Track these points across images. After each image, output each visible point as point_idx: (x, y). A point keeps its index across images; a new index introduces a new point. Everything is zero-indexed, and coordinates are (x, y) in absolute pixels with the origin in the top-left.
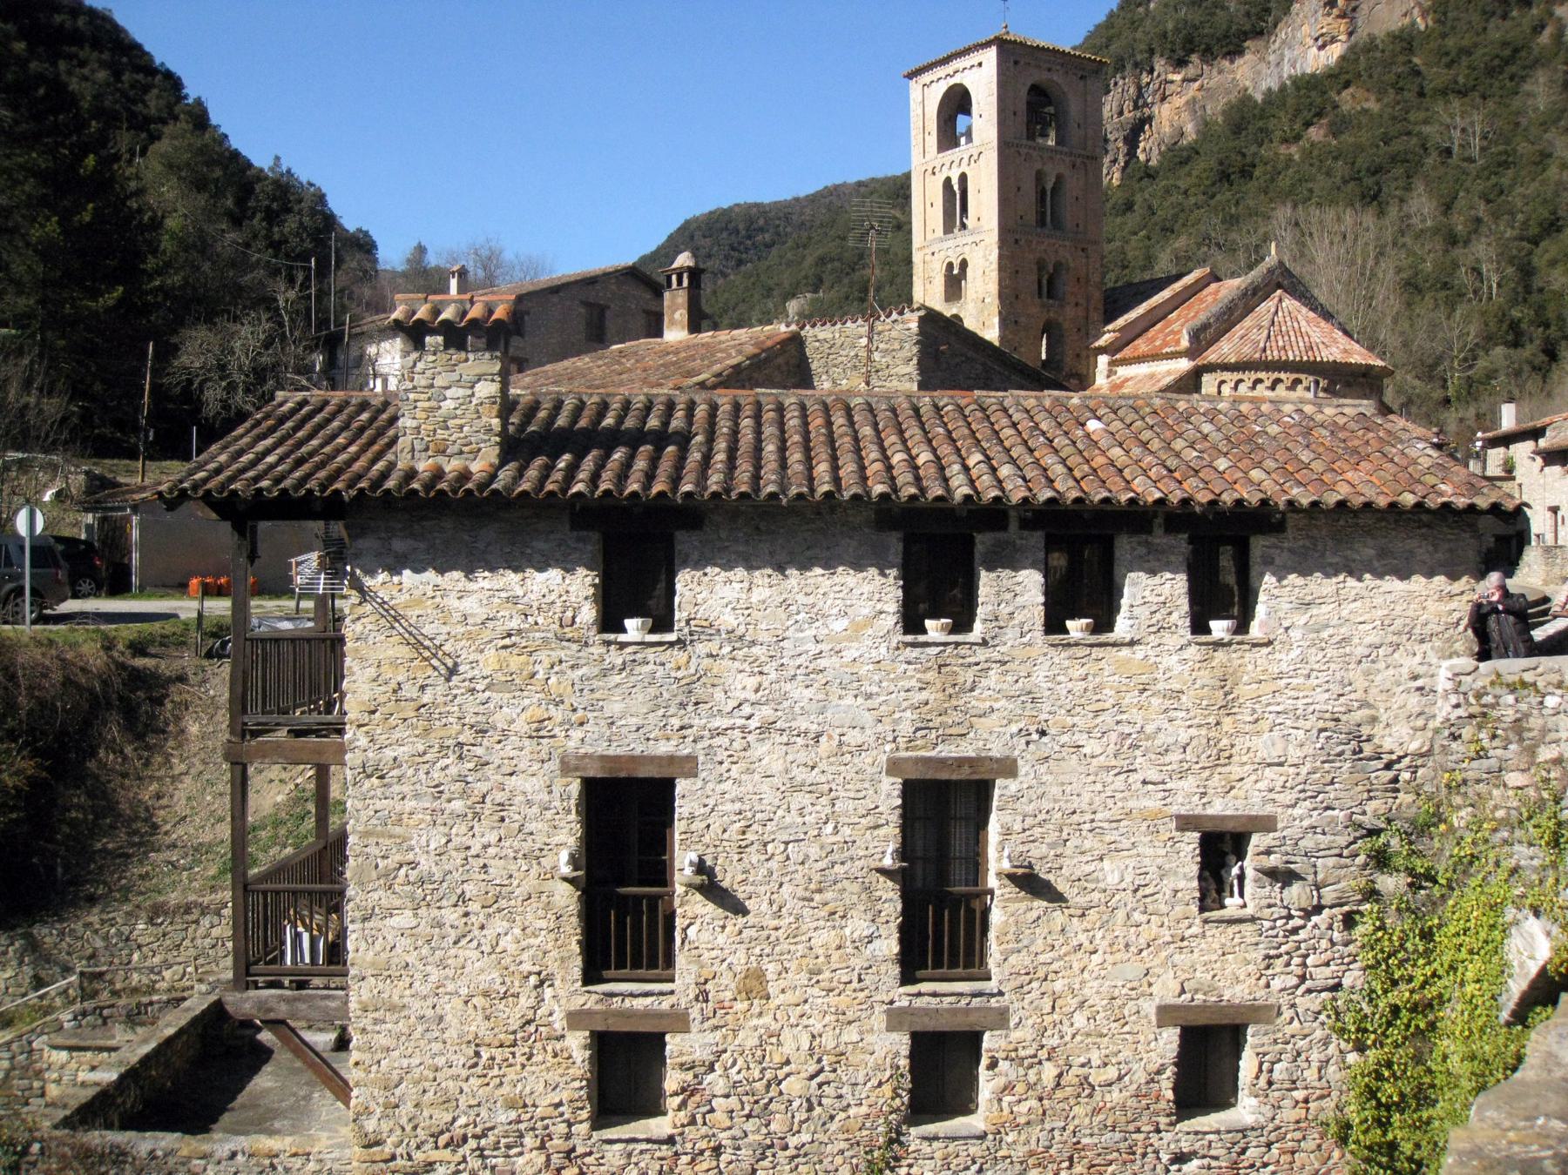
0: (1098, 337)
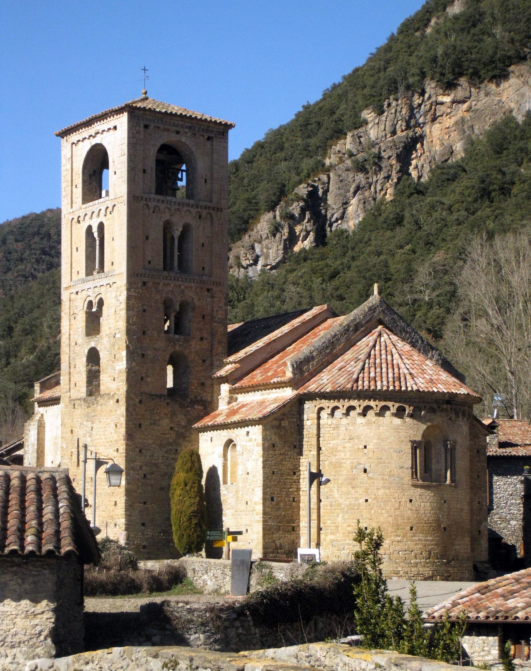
0: (222, 366)
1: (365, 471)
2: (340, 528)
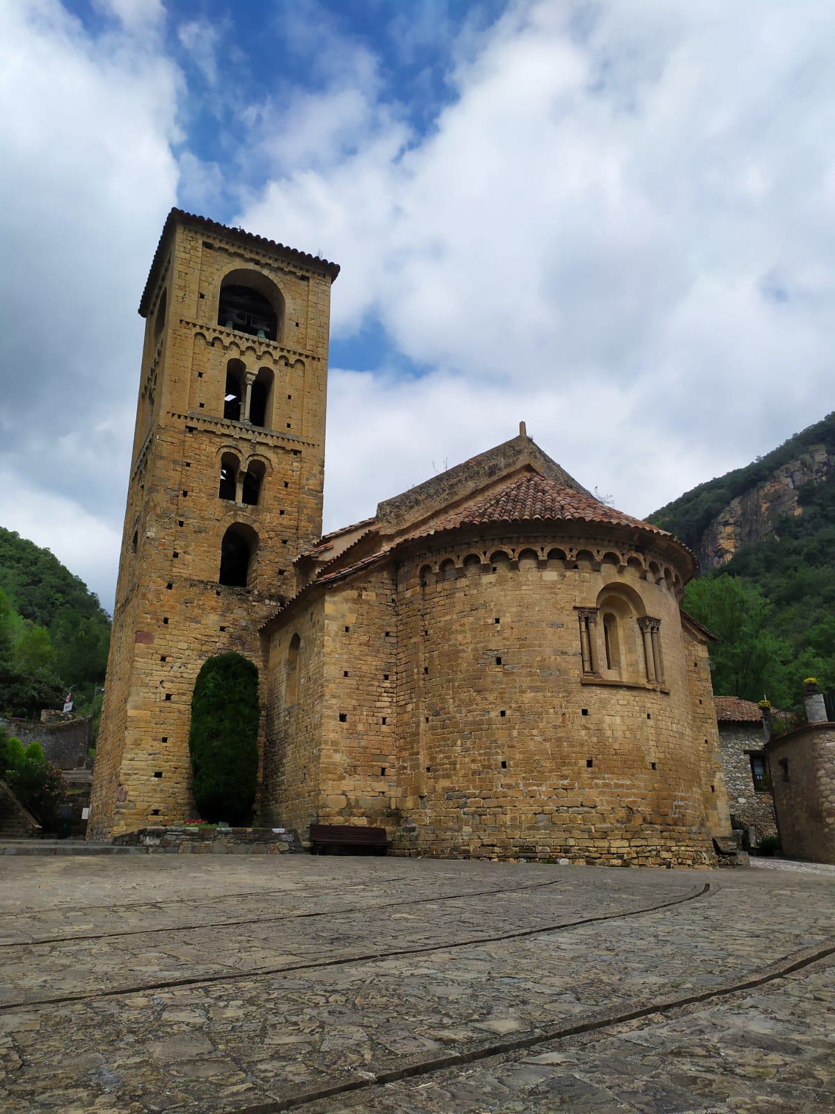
1: (499, 661)
2: (458, 766)
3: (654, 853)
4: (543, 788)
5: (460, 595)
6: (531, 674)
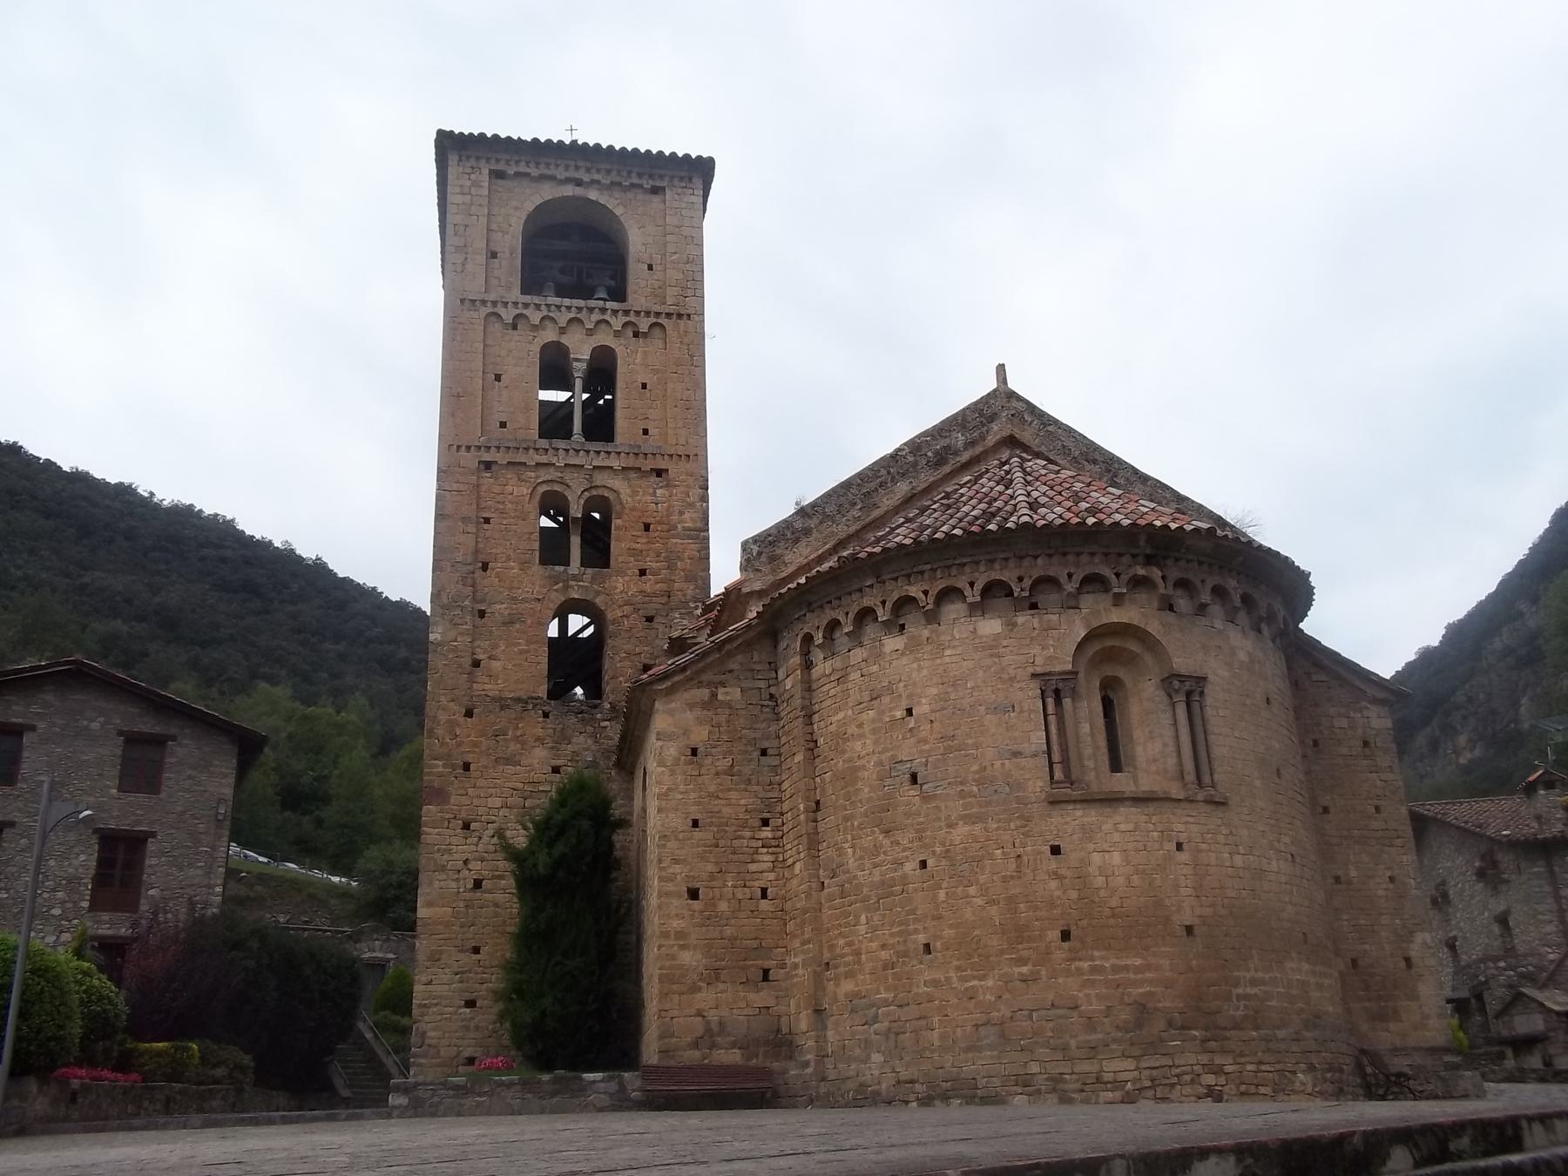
1: (914, 778)
3: (1188, 1078)
4: (990, 983)
5: (855, 676)
6: (962, 795)
